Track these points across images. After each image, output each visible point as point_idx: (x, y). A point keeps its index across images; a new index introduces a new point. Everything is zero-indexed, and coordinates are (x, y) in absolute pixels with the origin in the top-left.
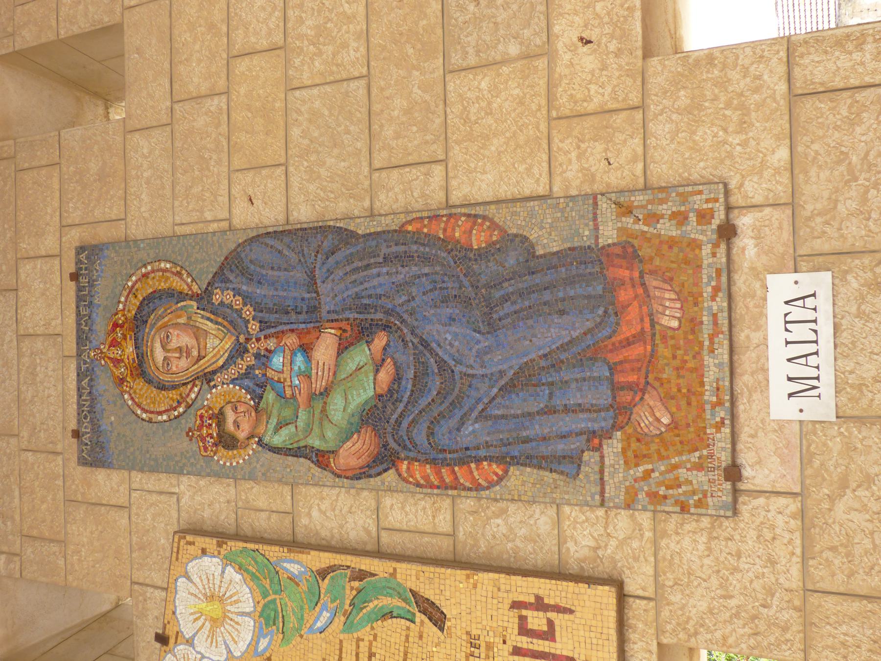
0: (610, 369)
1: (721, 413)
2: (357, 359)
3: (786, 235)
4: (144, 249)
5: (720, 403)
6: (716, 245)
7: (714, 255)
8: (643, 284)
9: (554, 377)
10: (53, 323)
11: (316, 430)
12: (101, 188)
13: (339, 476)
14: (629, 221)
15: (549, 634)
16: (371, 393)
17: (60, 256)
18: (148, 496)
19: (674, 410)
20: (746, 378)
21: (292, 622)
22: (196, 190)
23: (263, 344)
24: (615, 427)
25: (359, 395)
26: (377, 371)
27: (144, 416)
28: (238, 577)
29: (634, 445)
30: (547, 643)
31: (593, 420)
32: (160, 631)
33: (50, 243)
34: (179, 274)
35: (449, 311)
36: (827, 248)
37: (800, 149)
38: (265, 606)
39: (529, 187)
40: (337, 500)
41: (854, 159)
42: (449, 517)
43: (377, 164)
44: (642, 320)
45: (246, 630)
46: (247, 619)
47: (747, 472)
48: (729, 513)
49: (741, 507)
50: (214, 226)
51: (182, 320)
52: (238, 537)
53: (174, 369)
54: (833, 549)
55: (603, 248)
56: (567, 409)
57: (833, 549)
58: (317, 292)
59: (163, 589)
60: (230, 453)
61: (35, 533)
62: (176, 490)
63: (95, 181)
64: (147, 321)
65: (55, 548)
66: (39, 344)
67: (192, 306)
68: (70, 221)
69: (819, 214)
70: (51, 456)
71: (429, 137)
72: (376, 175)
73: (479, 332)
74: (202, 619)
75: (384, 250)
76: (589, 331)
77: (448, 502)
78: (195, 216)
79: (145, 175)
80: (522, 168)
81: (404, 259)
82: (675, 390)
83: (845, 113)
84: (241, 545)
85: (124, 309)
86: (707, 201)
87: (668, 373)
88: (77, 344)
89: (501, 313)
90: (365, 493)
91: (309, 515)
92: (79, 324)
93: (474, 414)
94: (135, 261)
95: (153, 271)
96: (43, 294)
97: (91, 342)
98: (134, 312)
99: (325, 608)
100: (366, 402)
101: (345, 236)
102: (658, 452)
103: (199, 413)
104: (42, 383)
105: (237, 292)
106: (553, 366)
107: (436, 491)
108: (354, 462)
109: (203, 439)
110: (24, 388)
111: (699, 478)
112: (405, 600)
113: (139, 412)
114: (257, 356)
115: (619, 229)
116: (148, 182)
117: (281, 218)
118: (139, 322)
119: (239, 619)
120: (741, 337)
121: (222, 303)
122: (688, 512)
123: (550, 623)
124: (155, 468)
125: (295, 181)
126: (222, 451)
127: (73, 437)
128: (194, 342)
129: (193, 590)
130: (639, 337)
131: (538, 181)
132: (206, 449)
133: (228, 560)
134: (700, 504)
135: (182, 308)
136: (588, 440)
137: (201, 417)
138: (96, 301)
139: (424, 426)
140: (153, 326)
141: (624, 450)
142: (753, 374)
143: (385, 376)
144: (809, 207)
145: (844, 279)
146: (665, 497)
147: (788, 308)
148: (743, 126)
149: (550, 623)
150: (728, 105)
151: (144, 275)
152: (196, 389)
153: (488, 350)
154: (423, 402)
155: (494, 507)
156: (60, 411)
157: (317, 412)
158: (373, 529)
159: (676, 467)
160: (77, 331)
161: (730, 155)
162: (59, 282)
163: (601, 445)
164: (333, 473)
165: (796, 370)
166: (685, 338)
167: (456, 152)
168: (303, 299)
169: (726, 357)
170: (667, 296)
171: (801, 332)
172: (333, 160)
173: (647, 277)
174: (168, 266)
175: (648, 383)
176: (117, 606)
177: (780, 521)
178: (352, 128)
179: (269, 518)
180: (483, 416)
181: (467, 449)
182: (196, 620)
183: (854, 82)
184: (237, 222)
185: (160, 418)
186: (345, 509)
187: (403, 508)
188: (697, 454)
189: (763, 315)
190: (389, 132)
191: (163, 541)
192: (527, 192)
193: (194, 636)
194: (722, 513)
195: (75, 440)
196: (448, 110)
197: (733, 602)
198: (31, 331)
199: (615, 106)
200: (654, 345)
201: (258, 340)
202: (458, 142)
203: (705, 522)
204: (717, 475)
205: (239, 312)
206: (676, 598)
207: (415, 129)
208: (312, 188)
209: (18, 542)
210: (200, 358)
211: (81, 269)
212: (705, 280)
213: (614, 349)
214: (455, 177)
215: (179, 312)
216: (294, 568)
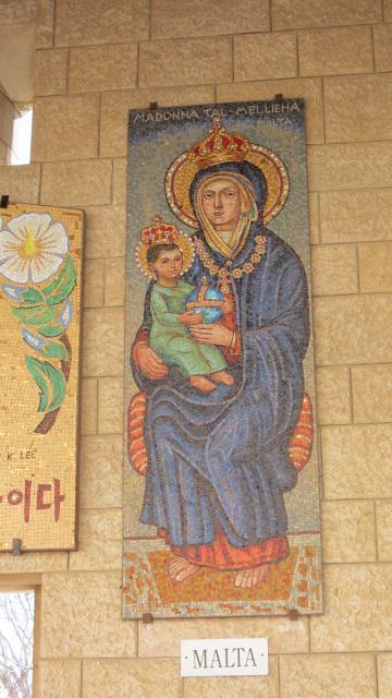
0: (209, 543)
1: (184, 612)
2: (214, 362)
3: (292, 649)
4: (299, 168)
5: (189, 611)
6: (285, 608)
7: (279, 607)
8: (261, 564)
9: (204, 504)
10: (243, 73)
11: (164, 329)
12: (351, 119)
13: (132, 349)
14: (302, 554)
15: (41, 506)
16: (191, 373)
17: (298, 77)
18: (109, 176)
19: (185, 583)
20: (205, 625)
21: (29, 315)
22: (345, 213)
23: (224, 282)
24: (173, 546)
25: (189, 363)
26: (206, 376)
27: (170, 175)
28: (55, 268)
29: (163, 558)
30: (35, 504)
31: (177, 533)
32: (10, 199)
33: (309, 67)
34: (279, 203)
35: (247, 432)
36: (282, 672)
37: (343, 657)
38: (38, 292)
39: (330, 485)
40: (116, 344)
41: (334, 688)
42: (110, 430)
43: (354, 370)
44: (240, 563)
45: (19, 277)
46: (27, 278)
47: (149, 626)
48: (124, 616)
49: (128, 622)
50: (315, 231)
51: (243, 209)
52: (84, 260)
53: (206, 202)
54: (107, 675)
55: (286, 538)
56: (183, 515)
57: (107, 675)
58: (262, 327)
59: (39, 201)
60: (145, 256)
61: (73, 63)
62: (114, 203)
63: (358, 111)
64: (242, 173)
65: (62, 84)
66: (226, 58)
67: (253, 217)
68: (326, 87)
69: (303, 669)
70: (134, 78)
71: (370, 411)
72: (346, 369)
73: (233, 453)
74: (22, 238)
75: (291, 381)
76: (233, 531)
77: (119, 429)
78: (324, 212)
79: (360, 162)
80: (344, 480)
81: (283, 394)
82: (197, 583)
83: (363, 683)
84: (79, 270)
85: (252, 151)
86: (312, 603)
87: (207, 579)
88: (226, 104)
89: (245, 469)
90: (121, 367)
91: (104, 321)
92: (241, 104)
93: (178, 451)
94: (291, 160)
95: (281, 178)
96: (267, 60)
97: (227, 118)
98: (249, 161)
99: (41, 341)
100: (184, 369)
101: (300, 350)
102: (158, 574)
103: (173, 226)
104: (194, 64)
105: (264, 259)
106: (211, 505)
107: (126, 423)
108: (143, 361)
109: (154, 231)
110: (189, 45)
111: (144, 599)
112: (52, 405)
113: (172, 169)
114: (216, 278)
115: (297, 548)
116: (354, 165)
117: (318, 292)
118: (243, 167)
119: (26, 270)
120: (230, 623)
121: (255, 244)
122: (122, 593)
123: (48, 506)
124: (130, 187)
125: (346, 302)
126: (146, 248)
127: (151, 104)
128: (226, 221)
129: (44, 228)
130: (230, 562)
131: (334, 491)
132: (147, 233)
133: (67, 259)
134: (128, 599)
135: (252, 207)
136: (164, 529)
137: (170, 229)
138: (259, 122)
139: (169, 413)
140: (238, 179)
141: (159, 552)
142: (208, 630)
143: (203, 384)
144: (308, 663)
145: (264, 681)
146: (131, 578)
147: (247, 650)
148: (359, 624)
149: (48, 506)
150: (373, 615)
151: (278, 168)
152: (191, 223)
153: (221, 459)
154: (185, 413)
155: (118, 464)
156: (172, 84)
157: (177, 329)
158: (97, 374)
159: (150, 584)
160: (235, 104)
161: (341, 616)
162: (277, 76)
163: (161, 537)
164: (135, 344)
165: (210, 655)
166: (229, 590)
167: (357, 432)
168: (257, 316)
169: (217, 614)
170: (255, 579)
171: (233, 658)
172: (359, 333)
173: (267, 566)
174: (285, 193)
175: (201, 566)
176: (12, 103)
177: (121, 645)
178: (382, 349)
179: (99, 287)
180: (176, 458)
181: (156, 446)
182: (21, 231)
183: (381, 688)
184: (318, 251)
185: (169, 190)
186: (110, 352)
187: (113, 396)
188: (158, 597)
189: (244, 636)
190: (377, 380)
191: (76, 191)
192: (327, 484)
193: (10, 231)
194: (124, 612)
195: (148, 105)
196: (387, 425)
197: (71, 617)
198: (236, 49)
199: (380, 544)
200: (224, 571)
201: (228, 277)
202: (364, 434)
203: (118, 602)
204: (146, 610)
205: (248, 260)
206: (71, 584)
207: (377, 400)
208: (340, 317)
209: (65, 45)
210: (215, 226)
211: (285, 105)
212: (264, 602)
213: (223, 545)
214: (340, 431)
215: (249, 205)
216: (66, 316)
